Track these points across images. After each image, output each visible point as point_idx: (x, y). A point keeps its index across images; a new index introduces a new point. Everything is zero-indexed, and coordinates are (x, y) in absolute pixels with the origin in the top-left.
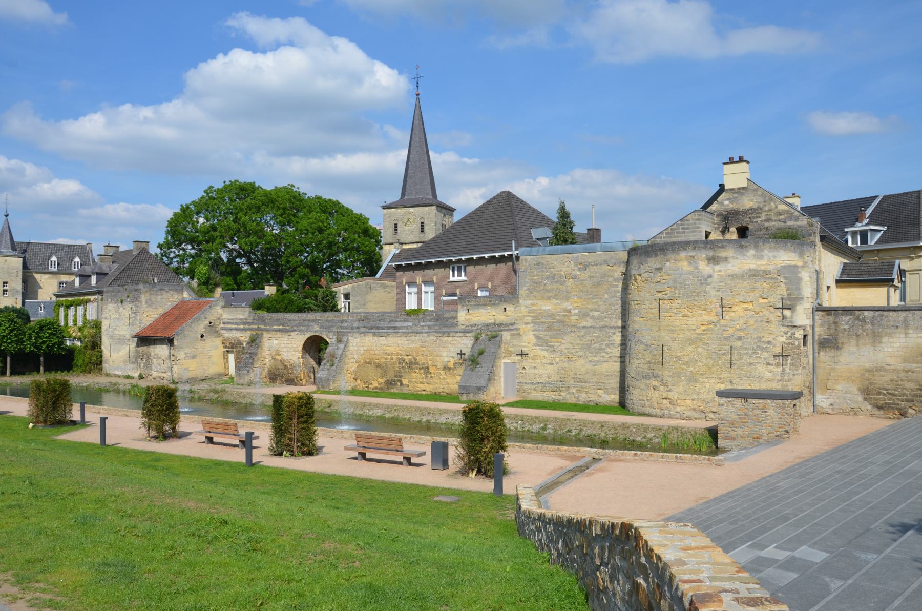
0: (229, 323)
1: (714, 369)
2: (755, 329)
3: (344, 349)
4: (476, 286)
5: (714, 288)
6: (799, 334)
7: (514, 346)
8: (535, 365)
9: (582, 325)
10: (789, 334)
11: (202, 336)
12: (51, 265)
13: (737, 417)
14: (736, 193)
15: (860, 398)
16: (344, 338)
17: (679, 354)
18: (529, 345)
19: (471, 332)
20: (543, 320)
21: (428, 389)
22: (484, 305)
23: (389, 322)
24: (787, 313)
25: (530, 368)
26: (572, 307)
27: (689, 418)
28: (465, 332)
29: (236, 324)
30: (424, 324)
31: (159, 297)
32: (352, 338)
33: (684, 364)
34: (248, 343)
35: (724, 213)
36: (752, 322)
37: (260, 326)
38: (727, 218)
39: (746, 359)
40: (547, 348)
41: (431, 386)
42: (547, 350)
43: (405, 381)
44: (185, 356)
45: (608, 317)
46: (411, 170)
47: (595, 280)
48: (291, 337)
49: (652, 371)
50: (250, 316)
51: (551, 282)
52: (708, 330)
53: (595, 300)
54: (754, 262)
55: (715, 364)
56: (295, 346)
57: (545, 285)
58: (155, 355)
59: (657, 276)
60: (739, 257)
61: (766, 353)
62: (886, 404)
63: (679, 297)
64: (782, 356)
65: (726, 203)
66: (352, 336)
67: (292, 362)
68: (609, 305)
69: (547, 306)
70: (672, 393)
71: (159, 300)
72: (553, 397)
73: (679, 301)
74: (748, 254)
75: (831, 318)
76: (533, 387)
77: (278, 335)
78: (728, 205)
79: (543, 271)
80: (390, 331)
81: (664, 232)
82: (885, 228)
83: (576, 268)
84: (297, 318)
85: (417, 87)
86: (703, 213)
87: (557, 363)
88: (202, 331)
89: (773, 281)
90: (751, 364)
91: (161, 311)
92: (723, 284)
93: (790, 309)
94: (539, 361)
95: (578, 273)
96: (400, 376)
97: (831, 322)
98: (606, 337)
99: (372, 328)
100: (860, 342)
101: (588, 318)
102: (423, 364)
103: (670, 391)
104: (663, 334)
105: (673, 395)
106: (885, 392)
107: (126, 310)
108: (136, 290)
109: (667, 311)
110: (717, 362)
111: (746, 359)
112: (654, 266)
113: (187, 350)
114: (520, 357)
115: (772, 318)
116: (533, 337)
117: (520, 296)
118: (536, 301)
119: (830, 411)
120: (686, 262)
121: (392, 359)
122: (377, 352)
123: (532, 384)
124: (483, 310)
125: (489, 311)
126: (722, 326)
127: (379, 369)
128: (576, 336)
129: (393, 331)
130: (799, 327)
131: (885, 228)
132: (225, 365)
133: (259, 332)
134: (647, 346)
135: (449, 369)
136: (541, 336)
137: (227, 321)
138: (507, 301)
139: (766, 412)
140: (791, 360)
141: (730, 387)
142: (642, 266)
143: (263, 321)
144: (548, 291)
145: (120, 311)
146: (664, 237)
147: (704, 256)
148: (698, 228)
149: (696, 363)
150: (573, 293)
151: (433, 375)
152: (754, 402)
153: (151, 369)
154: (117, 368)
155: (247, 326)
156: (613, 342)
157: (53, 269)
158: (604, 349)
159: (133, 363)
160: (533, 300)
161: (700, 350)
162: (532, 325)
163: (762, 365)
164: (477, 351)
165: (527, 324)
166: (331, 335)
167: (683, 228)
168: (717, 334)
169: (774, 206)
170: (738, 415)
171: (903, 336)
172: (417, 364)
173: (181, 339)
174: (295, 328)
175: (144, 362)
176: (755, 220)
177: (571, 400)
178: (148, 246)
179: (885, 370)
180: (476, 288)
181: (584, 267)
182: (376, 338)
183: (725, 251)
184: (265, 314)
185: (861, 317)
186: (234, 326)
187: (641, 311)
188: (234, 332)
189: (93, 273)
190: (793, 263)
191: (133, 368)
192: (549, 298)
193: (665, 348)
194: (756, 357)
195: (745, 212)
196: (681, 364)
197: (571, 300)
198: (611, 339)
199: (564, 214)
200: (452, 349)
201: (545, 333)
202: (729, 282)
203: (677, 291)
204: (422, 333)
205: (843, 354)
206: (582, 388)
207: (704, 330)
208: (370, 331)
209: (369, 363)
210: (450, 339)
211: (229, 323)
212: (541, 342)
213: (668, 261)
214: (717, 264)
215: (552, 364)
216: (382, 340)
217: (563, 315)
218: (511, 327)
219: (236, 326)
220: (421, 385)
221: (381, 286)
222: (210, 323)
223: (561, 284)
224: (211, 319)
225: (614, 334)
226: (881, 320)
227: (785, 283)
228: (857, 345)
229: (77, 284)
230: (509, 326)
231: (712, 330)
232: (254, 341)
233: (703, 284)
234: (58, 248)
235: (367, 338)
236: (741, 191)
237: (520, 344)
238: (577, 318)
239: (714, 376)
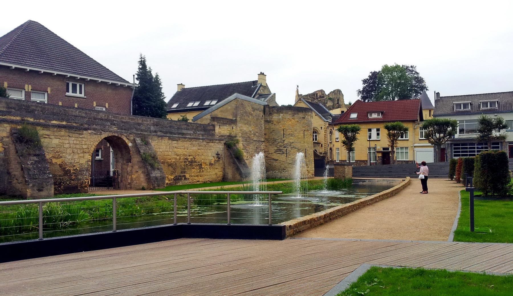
4: (95, 103)
9: (254, 139)
19: (223, 140)
20: (244, 136)
21: (200, 180)
28: (220, 140)
41: (202, 178)
42: (246, 152)
43: (187, 176)
48: (81, 136)
69: (245, 128)
84: (84, 115)
96: (184, 172)
102: (199, 162)
112: (301, 116)
127: (170, 168)
134: (298, 149)
135: (212, 164)
144: (245, 120)
165: (240, 137)
172: (195, 162)
182: (170, 141)
192: (245, 124)
201: (245, 143)
204: (200, 139)
208: (165, 135)
210: (212, 144)
213: (306, 115)
220: (196, 178)
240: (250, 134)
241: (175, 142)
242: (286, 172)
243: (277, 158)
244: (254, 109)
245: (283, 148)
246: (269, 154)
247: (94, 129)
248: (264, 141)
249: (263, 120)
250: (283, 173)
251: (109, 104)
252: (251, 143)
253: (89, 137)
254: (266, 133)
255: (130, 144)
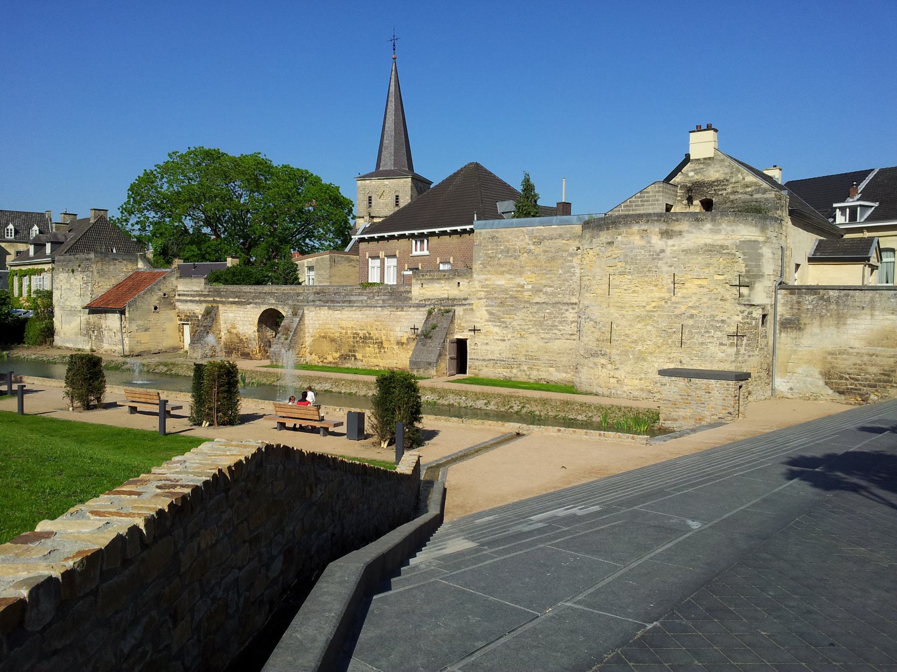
0: (184, 295)
1: (664, 348)
2: (708, 308)
3: (299, 322)
4: (438, 259)
5: (667, 263)
6: (757, 313)
7: (466, 321)
8: (486, 341)
9: (535, 301)
10: (746, 313)
11: (156, 308)
12: (8, 233)
13: (680, 397)
14: (702, 163)
15: (821, 383)
16: (299, 311)
17: (627, 332)
18: (482, 321)
19: (425, 306)
20: (496, 295)
21: (381, 364)
22: (438, 279)
23: (345, 296)
24: (744, 291)
25: (483, 344)
26: (525, 283)
27: (636, 399)
28: (418, 306)
29: (192, 295)
30: (378, 298)
31: (112, 267)
32: (307, 312)
33: (632, 342)
34: (203, 316)
35: (689, 185)
36: (705, 300)
37: (215, 299)
38: (691, 192)
39: (698, 339)
40: (499, 324)
41: (384, 361)
42: (499, 326)
43: (359, 356)
44: (137, 328)
45: (561, 293)
46: (387, 140)
47: (550, 255)
48: (246, 310)
49: (600, 349)
50: (205, 288)
51: (505, 256)
52: (659, 307)
53: (548, 276)
54: (710, 236)
55: (664, 343)
56: (250, 319)
57: (499, 259)
58: (106, 326)
59: (610, 251)
60: (694, 230)
61: (719, 333)
62: (848, 389)
63: (629, 272)
64: (737, 336)
65: (691, 174)
66: (308, 309)
67: (247, 336)
68: (563, 280)
69: (501, 281)
70: (619, 371)
71: (111, 270)
72: (505, 374)
73: (630, 277)
74: (704, 228)
75: (794, 297)
76: (485, 363)
77: (234, 308)
78: (692, 177)
79: (497, 245)
80: (345, 305)
81: (623, 205)
82: (877, 204)
83: (531, 242)
85: (394, 49)
86: (665, 185)
87: (509, 340)
88: (156, 303)
89: (730, 257)
90: (702, 344)
91: (114, 282)
92: (676, 259)
93: (748, 286)
94: (491, 337)
95: (533, 247)
96: (354, 351)
97: (795, 301)
98: (559, 314)
99: (327, 302)
100: (823, 323)
101: (541, 294)
103: (617, 369)
104: (612, 310)
105: (621, 374)
106: (847, 376)
107: (78, 280)
108: (87, 259)
109: (617, 287)
110: (667, 341)
111: (698, 339)
113: (140, 322)
114: (472, 333)
115: (727, 296)
116: (486, 313)
117: (473, 271)
118: (489, 276)
119: (789, 396)
120: (639, 236)
121: (346, 333)
122: (332, 326)
123: (484, 360)
124: (437, 285)
125: (443, 285)
126: (673, 303)
128: (529, 312)
129: (348, 305)
130: (758, 306)
131: (877, 204)
132: (180, 338)
133: (215, 305)
135: (403, 344)
136: (494, 311)
137: (182, 293)
138: (461, 275)
139: (709, 393)
140: (747, 340)
141: (680, 367)
142: (594, 240)
143: (218, 293)
144: (502, 266)
145: (72, 281)
146: (622, 210)
147: (657, 230)
148: (658, 200)
149: (645, 341)
150: (527, 268)
151: (386, 350)
152: (697, 382)
153: (103, 342)
154: (68, 341)
155: (202, 299)
156: (565, 319)
157: (9, 237)
158: (557, 326)
159: (85, 335)
160: (486, 274)
161: (649, 328)
162: (485, 300)
163: (714, 345)
164: (430, 326)
166: (286, 308)
167: (642, 201)
168: (668, 312)
169: (741, 177)
170: (681, 395)
171: (869, 317)
172: (371, 338)
173: (133, 310)
174: (251, 301)
175: (96, 334)
176: (720, 193)
177: (522, 378)
178: (107, 214)
179: (848, 354)
180: (438, 263)
181: (539, 241)
182: (331, 312)
183: (679, 224)
184: (222, 287)
185: (825, 297)
186: (189, 298)
187: (592, 287)
188: (189, 304)
189: (48, 242)
190: (753, 238)
191: (84, 341)
192: (503, 273)
193: (614, 326)
194: (709, 337)
195: (711, 184)
196: (630, 342)
197: (525, 275)
198: (564, 315)
199: (528, 187)
200: (406, 324)
201: (498, 308)
202: (683, 257)
203: (628, 267)
204: (376, 307)
205: (805, 336)
206: (534, 365)
207: (654, 307)
208: (325, 304)
209: (324, 337)
210: (403, 313)
211: (184, 295)
212: (494, 317)
213: (619, 234)
214: (671, 238)
215: (504, 340)
216: (337, 314)
217: (516, 291)
218: (464, 302)
219: (191, 298)
220: (375, 360)
221: (346, 260)
222: (165, 295)
223: (515, 258)
224: (166, 290)
225: (567, 310)
226: (847, 300)
227: (743, 260)
228: (821, 326)
229: (32, 253)
230: (462, 301)
231: (663, 307)
232: (211, 314)
233: (655, 258)
234: (14, 216)
235: (322, 312)
236: (707, 161)
237: (473, 320)
238: (530, 293)
239: (664, 355)
241: (339, 312)
247: (255, 303)
251: (454, 258)
252: (518, 309)
253: (252, 310)
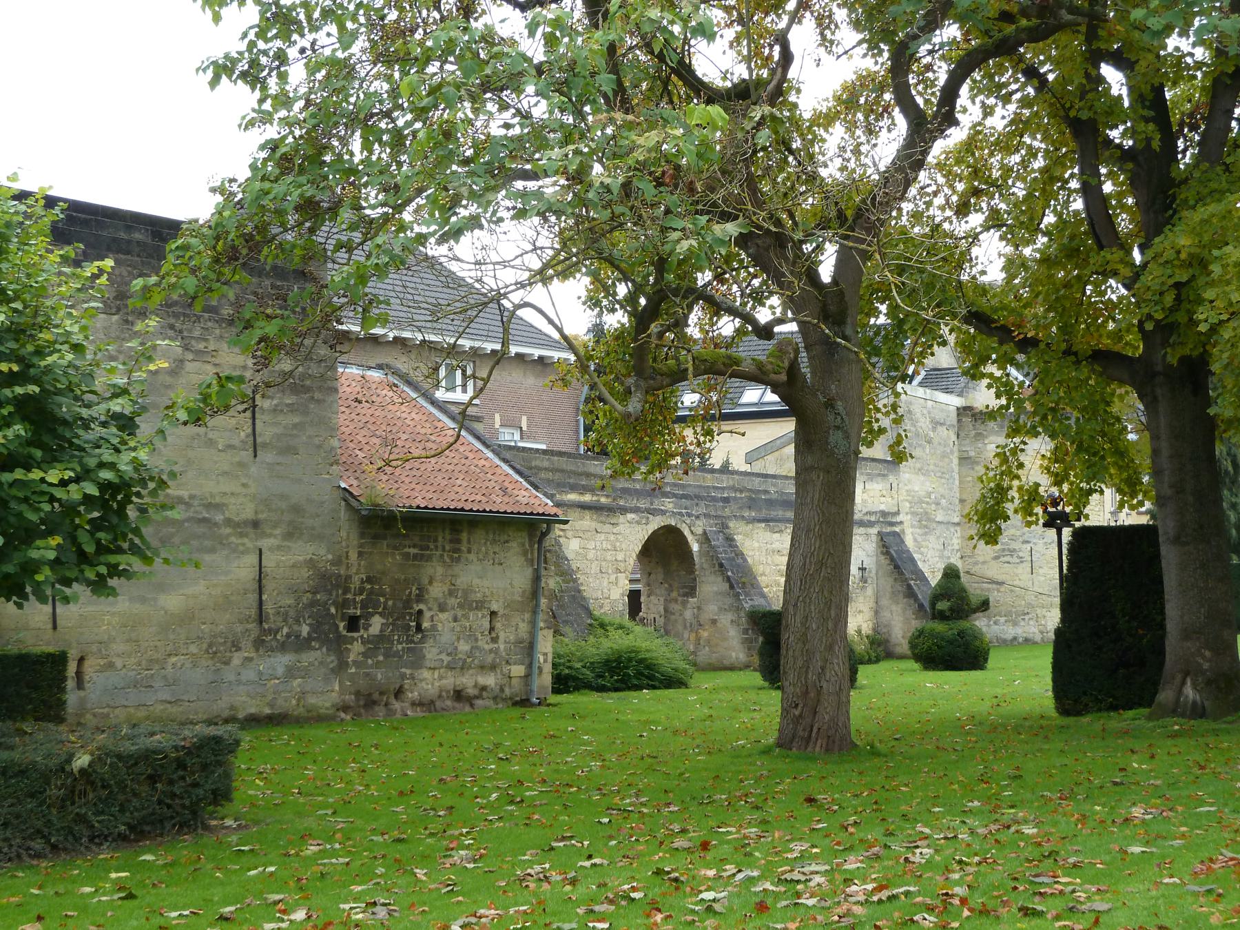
4: (497, 417)
56: (620, 557)
240: (928, 503)
242: (1031, 623)
243: (1000, 578)
244: (936, 424)
245: (1021, 545)
246: (976, 563)
248: (958, 524)
249: (956, 454)
250: (1022, 623)
254: (964, 497)
255: (695, 547)
